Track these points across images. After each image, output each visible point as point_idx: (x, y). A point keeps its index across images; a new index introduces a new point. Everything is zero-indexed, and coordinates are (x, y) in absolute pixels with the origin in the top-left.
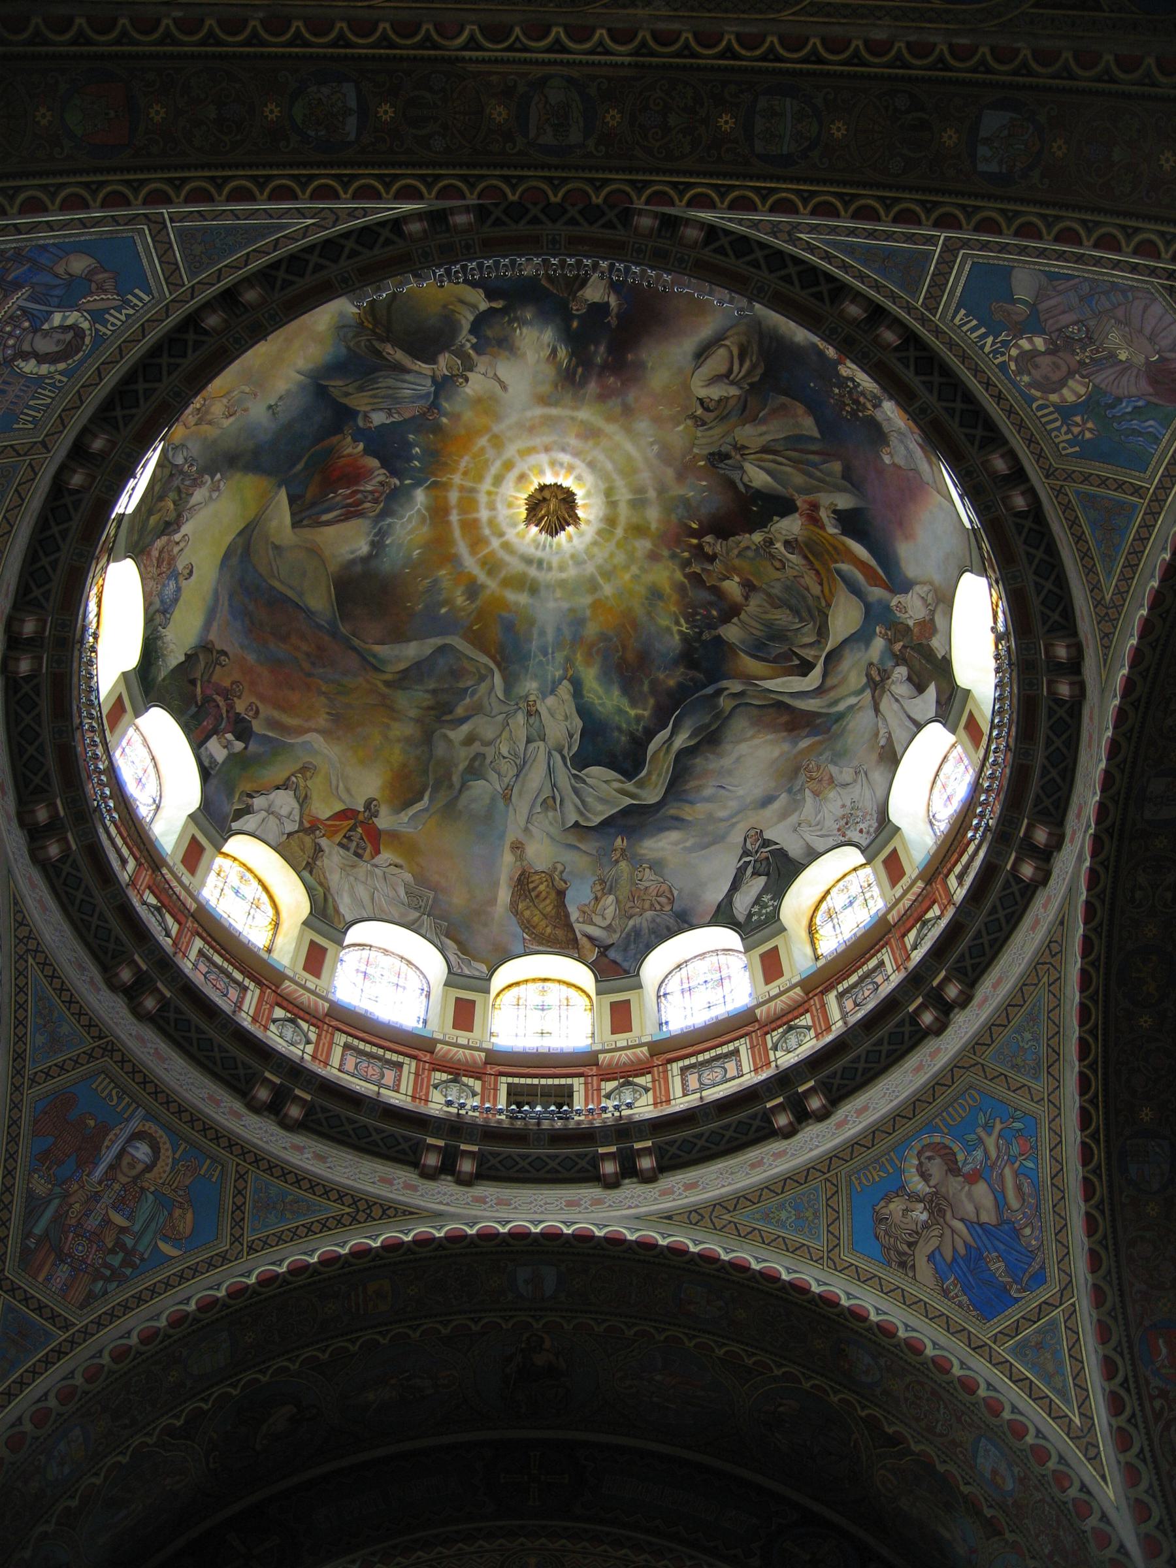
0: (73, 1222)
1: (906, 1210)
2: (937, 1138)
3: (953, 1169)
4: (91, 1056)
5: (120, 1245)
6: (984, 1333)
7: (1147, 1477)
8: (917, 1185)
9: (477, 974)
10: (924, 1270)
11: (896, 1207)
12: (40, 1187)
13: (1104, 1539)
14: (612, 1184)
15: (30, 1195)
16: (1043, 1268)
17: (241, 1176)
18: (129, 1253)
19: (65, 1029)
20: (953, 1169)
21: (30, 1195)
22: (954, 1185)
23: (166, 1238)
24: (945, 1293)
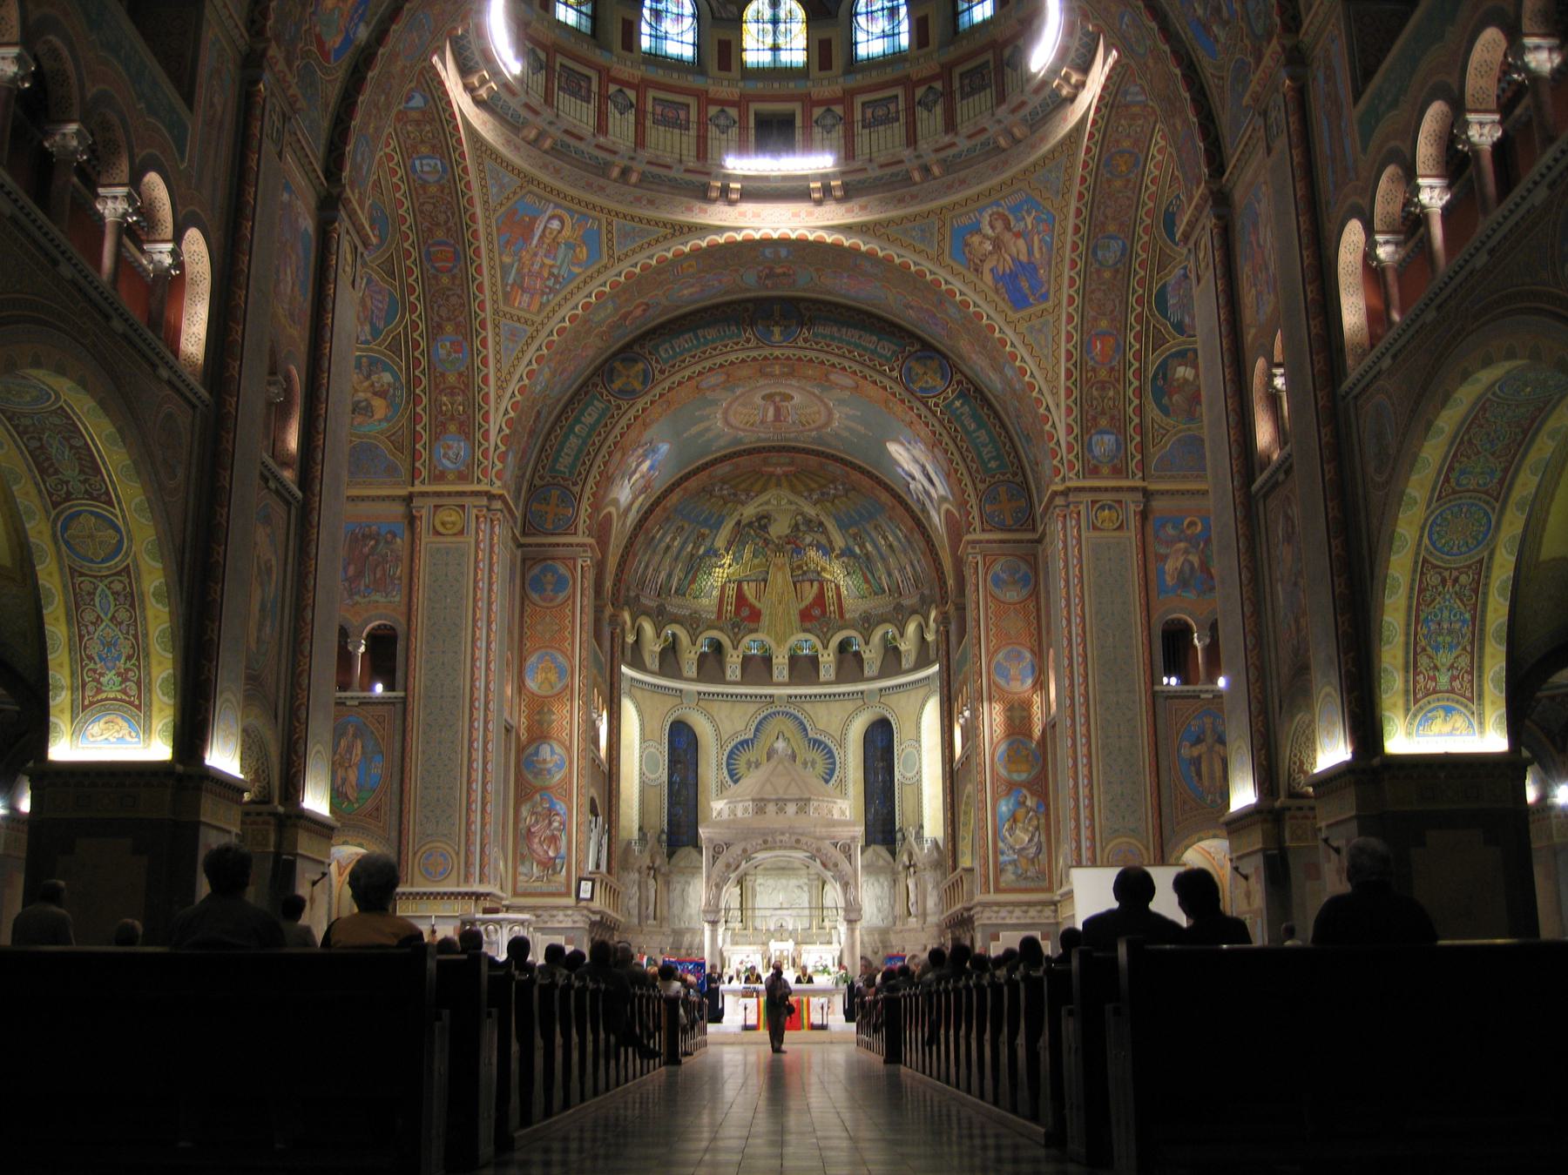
0: (526, 270)
1: (981, 243)
2: (1000, 210)
3: (1008, 227)
4: (521, 187)
5: (551, 274)
6: (1013, 316)
7: (1076, 411)
8: (989, 232)
9: (731, 16)
10: (988, 277)
11: (976, 239)
12: (507, 260)
13: (1051, 437)
14: (819, 202)
15: (502, 266)
16: (1048, 291)
17: (609, 224)
18: (556, 277)
19: (506, 180)
20: (1008, 227)
21: (502, 266)
22: (1007, 236)
23: (574, 264)
24: (997, 291)
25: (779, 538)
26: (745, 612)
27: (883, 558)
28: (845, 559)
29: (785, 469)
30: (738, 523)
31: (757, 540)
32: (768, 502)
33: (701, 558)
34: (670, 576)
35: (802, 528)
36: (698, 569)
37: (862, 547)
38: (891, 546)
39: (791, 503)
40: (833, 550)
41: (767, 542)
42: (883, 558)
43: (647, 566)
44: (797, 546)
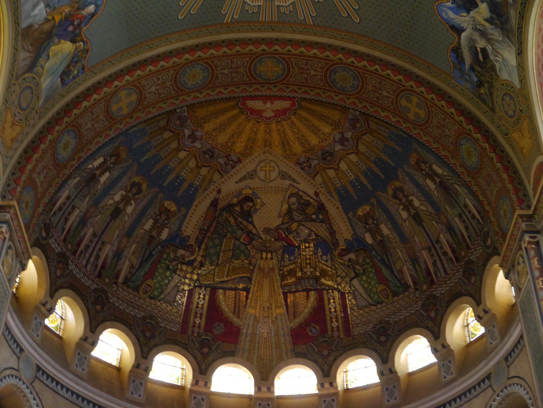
25: (267, 231)
26: (219, 329)
27: (404, 239)
28: (352, 256)
29: (279, 105)
30: (214, 203)
31: (239, 232)
32: (252, 175)
33: (165, 245)
34: (118, 255)
35: (297, 216)
36: (158, 261)
37: (375, 231)
38: (417, 218)
39: (283, 175)
40: (336, 244)
41: (251, 237)
42: (404, 239)
43: (83, 221)
44: (291, 244)
